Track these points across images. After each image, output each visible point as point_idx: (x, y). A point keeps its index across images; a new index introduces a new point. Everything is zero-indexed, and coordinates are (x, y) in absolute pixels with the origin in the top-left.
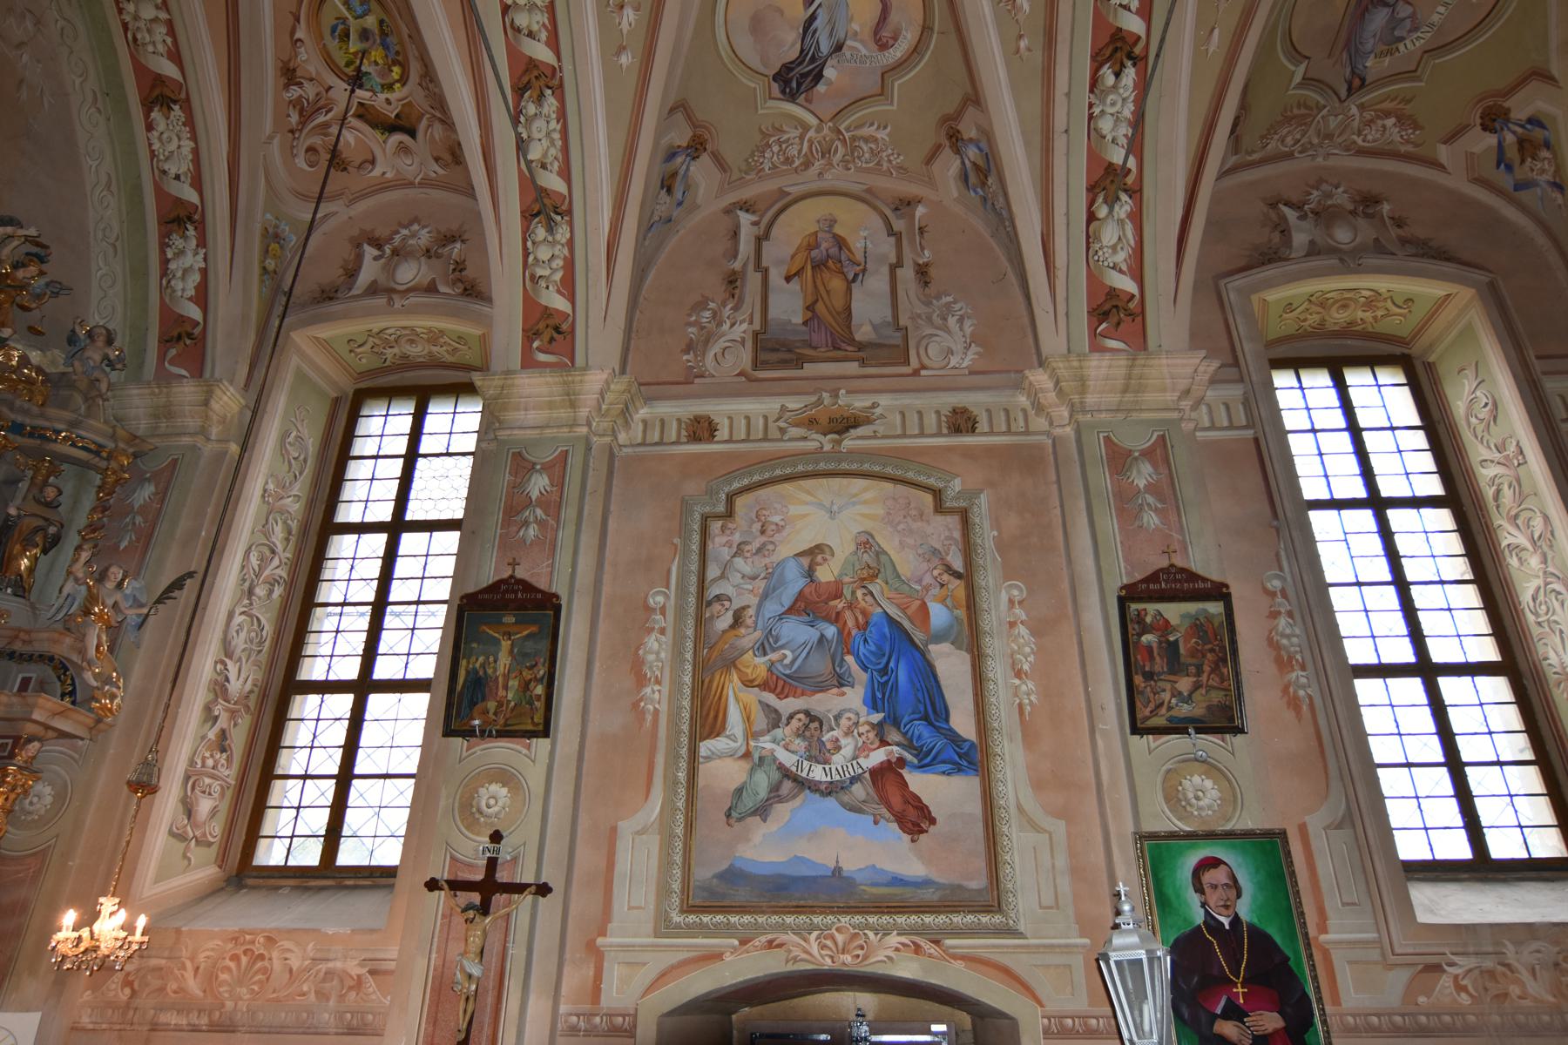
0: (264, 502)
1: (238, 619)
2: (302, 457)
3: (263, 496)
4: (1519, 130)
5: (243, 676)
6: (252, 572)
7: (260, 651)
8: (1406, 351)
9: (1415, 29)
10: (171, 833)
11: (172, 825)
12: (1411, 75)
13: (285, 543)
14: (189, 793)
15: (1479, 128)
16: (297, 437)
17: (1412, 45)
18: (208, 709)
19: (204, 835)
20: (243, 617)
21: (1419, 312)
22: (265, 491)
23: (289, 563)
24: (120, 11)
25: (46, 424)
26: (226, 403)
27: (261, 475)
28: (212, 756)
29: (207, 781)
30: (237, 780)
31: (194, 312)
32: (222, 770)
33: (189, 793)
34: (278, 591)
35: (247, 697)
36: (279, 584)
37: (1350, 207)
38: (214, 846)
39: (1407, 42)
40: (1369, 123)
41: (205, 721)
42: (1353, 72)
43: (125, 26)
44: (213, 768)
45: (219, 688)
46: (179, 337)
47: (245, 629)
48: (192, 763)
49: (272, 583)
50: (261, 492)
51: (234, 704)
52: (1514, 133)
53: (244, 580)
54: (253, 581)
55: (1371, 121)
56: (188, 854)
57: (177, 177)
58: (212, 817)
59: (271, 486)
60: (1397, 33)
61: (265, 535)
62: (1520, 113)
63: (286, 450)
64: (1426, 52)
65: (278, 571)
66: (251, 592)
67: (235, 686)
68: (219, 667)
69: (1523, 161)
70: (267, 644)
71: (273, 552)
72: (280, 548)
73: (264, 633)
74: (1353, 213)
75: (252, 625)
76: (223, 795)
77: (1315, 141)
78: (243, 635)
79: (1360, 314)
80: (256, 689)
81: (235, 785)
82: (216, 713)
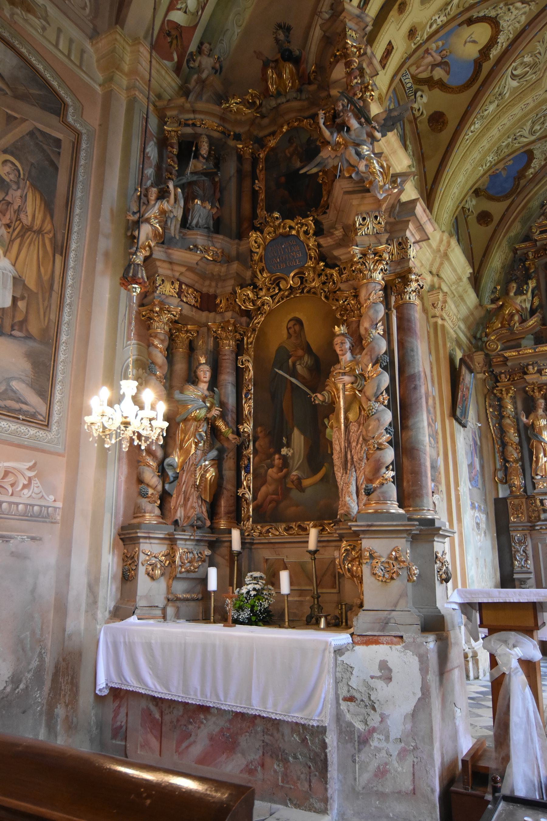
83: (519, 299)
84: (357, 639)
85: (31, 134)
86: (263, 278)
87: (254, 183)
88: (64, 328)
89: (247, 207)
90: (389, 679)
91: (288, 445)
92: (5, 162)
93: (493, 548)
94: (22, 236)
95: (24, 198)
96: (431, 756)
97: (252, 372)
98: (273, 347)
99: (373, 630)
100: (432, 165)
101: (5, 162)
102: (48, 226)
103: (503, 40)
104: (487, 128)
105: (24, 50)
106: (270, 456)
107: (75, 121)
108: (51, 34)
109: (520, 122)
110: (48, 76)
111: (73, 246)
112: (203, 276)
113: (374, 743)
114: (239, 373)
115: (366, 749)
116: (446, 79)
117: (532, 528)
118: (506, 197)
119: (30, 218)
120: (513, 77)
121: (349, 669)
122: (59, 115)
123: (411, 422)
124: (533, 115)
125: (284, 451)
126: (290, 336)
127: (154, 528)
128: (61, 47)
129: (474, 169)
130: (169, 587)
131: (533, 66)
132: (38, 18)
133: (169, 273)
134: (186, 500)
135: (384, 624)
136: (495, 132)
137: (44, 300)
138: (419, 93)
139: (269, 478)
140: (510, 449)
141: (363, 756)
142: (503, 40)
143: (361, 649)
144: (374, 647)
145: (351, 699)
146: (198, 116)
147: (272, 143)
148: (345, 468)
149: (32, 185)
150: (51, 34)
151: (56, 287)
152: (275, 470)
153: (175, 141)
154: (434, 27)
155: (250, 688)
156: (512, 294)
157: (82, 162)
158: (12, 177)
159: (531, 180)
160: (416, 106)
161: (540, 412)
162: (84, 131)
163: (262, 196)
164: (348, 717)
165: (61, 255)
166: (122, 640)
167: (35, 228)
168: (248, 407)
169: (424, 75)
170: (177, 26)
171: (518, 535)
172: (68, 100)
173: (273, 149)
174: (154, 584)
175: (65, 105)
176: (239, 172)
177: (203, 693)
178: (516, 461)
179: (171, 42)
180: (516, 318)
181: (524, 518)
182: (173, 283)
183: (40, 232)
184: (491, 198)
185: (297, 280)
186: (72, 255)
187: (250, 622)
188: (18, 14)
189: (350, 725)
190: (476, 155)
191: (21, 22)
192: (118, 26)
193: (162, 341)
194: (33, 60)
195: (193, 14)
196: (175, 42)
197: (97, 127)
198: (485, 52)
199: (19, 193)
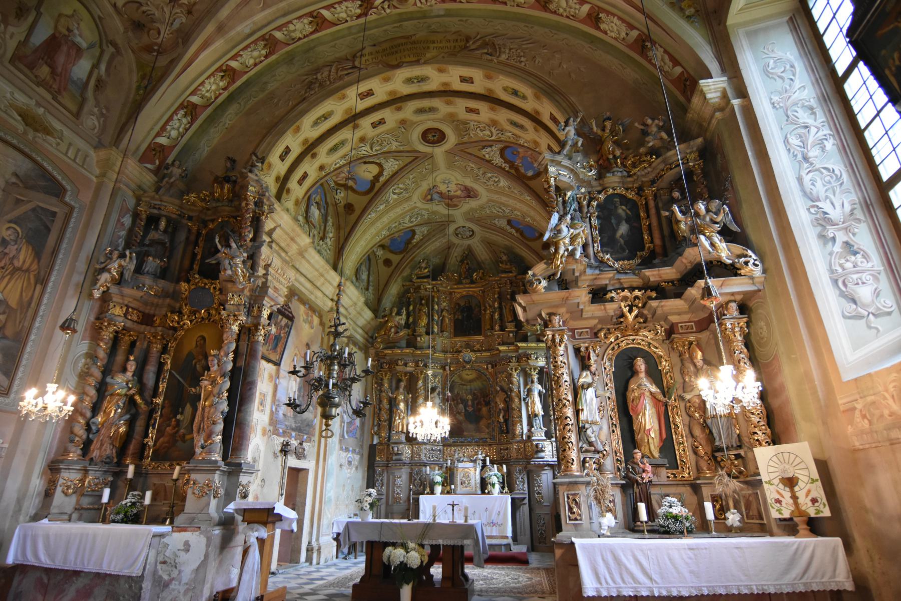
0: (777, 109)
1: (807, 179)
2: (788, 67)
3: (774, 107)
5: (838, 205)
6: (798, 148)
7: (841, 184)
10: (844, 317)
11: (843, 312)
13: (813, 116)
14: (844, 289)
16: (775, 62)
18: (822, 237)
19: (878, 309)
20: (811, 175)
22: (773, 104)
23: (826, 124)
24: (562, 15)
25: (658, 171)
26: (715, 89)
27: (763, 99)
28: (847, 261)
29: (855, 276)
30: (883, 265)
31: (678, 70)
32: (864, 265)
33: (844, 289)
34: (830, 145)
35: (852, 214)
36: (826, 139)
38: (893, 314)
41: (825, 244)
43: (568, 17)
44: (854, 267)
45: (823, 221)
46: (685, 85)
47: (818, 179)
48: (832, 271)
49: (821, 144)
50: (771, 106)
51: (843, 223)
53: (796, 156)
54: (802, 152)
56: (872, 325)
57: (627, 34)
58: (878, 295)
59: (775, 98)
61: (792, 123)
63: (772, 73)
65: (821, 133)
66: (806, 158)
67: (835, 214)
68: (812, 210)
70: (845, 177)
71: (807, 127)
72: (810, 121)
73: (837, 172)
75: (822, 173)
76: (876, 279)
78: (819, 184)
80: (858, 206)
81: (885, 270)
82: (832, 235)
83: (398, 318)
84: (175, 529)
85: (34, 210)
86: (186, 310)
87: (195, 248)
88: (34, 331)
89: (187, 263)
90: (187, 550)
91: (182, 413)
92: (8, 228)
93: (363, 478)
94: (12, 274)
95: (19, 251)
96: (202, 591)
97: (169, 365)
98: (186, 352)
99: (184, 523)
100: (343, 234)
101: (8, 228)
102: (35, 267)
103: (386, 175)
104: (379, 218)
105: (39, 159)
106: (169, 419)
107: (70, 200)
108: (63, 147)
109: (402, 215)
110: (55, 173)
111: (53, 279)
112: (146, 303)
113: (172, 586)
114: (161, 366)
115: (167, 590)
116: (354, 186)
117: (387, 466)
118: (401, 253)
119: (21, 263)
120: (394, 193)
121: (166, 546)
122: (57, 196)
123: (243, 408)
124: (410, 213)
125: (179, 417)
126: (197, 346)
127: (74, 462)
128: (69, 155)
129: (372, 238)
130: (78, 501)
131: (406, 189)
132: (55, 138)
133: (121, 301)
134: (102, 445)
135: (192, 520)
136: (385, 219)
137: (21, 314)
138: (339, 191)
139: (166, 433)
140: (383, 412)
141: (164, 594)
142: (386, 175)
143: (176, 535)
144: (183, 533)
145: (164, 562)
146: (163, 203)
147: (211, 226)
148: (198, 432)
149: (27, 241)
150: (63, 147)
151: (33, 305)
152: (170, 428)
153: (144, 216)
154: (338, 165)
155: (103, 559)
156: (394, 314)
157: (71, 225)
158: (12, 237)
159: (414, 246)
160: (337, 197)
161: (401, 390)
162: (77, 206)
163: (199, 257)
164: (160, 573)
165: (42, 285)
166: (30, 534)
167: (24, 268)
168: (162, 386)
169: (341, 182)
170: (161, 146)
171: (379, 470)
172: (68, 187)
173: (211, 230)
174: (67, 499)
175: (65, 190)
176: (187, 238)
177: (75, 563)
178: (385, 421)
179: (155, 154)
180: (393, 330)
181: (384, 459)
182: (121, 308)
183: (28, 270)
184: (391, 252)
185: (206, 314)
186: (50, 284)
187: (122, 521)
188: (39, 137)
189: (161, 577)
190: (373, 231)
191: (40, 141)
192: (114, 148)
193: (106, 344)
194: (45, 164)
195: (174, 139)
196: (158, 154)
197: (88, 203)
198: (377, 178)
199: (16, 247)
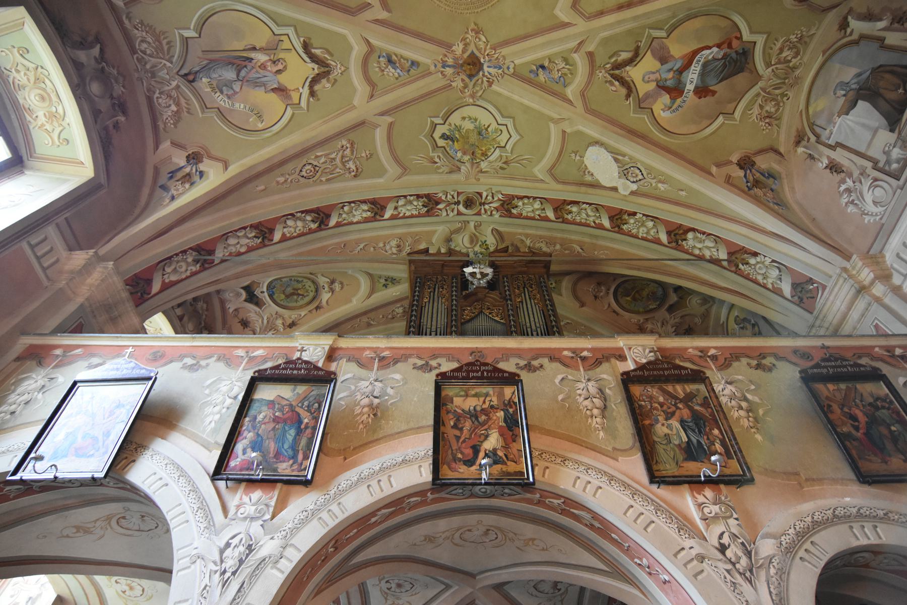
4: (194, 170)
8: (25, 158)
9: (229, 97)
12: (205, 107)
15: (187, 154)
17: (221, 100)
21: (62, 152)
37: (115, 95)
39: (221, 96)
40: (169, 96)
42: (196, 73)
52: (192, 169)
55: (171, 97)
60: (224, 88)
62: (202, 167)
64: (218, 109)
69: (178, 181)
74: (112, 97)
77: (148, 66)
79: (41, 114)
